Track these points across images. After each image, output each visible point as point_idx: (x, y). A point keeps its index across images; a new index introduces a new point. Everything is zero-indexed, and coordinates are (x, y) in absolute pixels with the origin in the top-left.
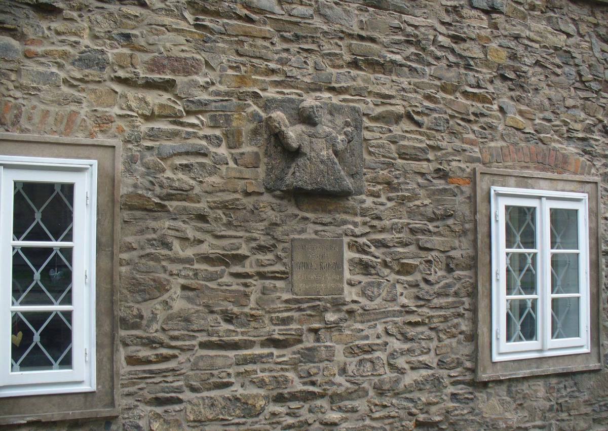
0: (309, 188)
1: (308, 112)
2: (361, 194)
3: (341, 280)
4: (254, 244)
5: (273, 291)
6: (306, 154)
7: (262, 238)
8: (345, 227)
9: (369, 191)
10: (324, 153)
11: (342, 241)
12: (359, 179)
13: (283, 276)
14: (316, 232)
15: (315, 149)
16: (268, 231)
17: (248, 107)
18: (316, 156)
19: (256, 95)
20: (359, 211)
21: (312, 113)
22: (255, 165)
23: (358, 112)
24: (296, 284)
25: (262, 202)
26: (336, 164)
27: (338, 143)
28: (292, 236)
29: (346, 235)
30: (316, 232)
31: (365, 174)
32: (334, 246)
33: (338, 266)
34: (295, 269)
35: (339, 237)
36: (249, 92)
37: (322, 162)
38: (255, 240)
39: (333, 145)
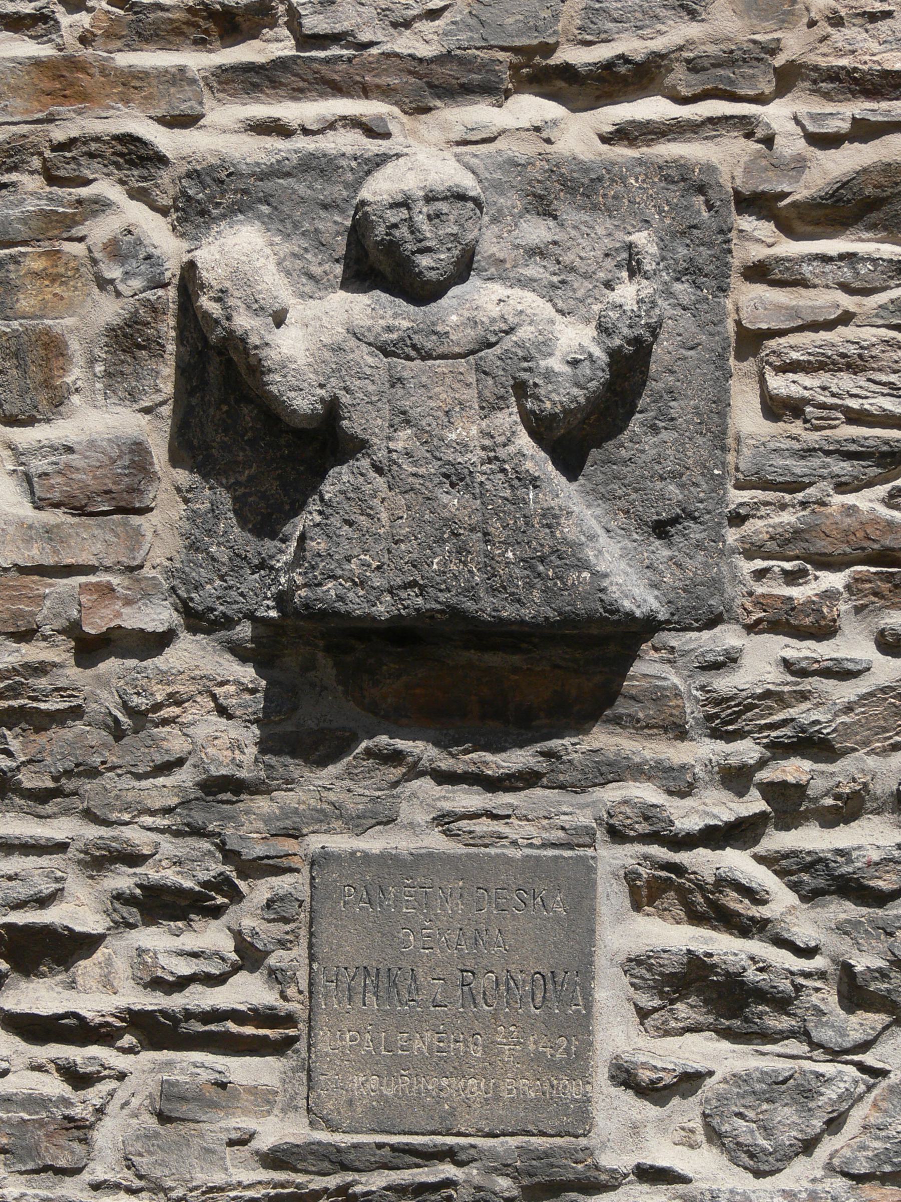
0: (383, 609)
1: (381, 230)
2: (713, 622)
3: (577, 1063)
4: (123, 880)
5: (213, 1105)
6: (360, 446)
7: (168, 846)
8: (612, 794)
9: (760, 602)
10: (467, 430)
11: (588, 868)
12: (699, 546)
13: (266, 1034)
14: (445, 821)
15: (414, 413)
16: (198, 817)
17: (94, 214)
18: (421, 452)
19: (134, 156)
20: (693, 712)
21: (403, 232)
22: (125, 500)
23: (701, 189)
25: (164, 677)
26: (535, 482)
27: (549, 375)
28: (315, 843)
29: (617, 835)
30: (445, 821)
31: (737, 519)
33: (564, 990)
34: (331, 1003)
35: (569, 846)
36: (97, 139)
37: (455, 478)
38: (133, 859)
39: (521, 389)
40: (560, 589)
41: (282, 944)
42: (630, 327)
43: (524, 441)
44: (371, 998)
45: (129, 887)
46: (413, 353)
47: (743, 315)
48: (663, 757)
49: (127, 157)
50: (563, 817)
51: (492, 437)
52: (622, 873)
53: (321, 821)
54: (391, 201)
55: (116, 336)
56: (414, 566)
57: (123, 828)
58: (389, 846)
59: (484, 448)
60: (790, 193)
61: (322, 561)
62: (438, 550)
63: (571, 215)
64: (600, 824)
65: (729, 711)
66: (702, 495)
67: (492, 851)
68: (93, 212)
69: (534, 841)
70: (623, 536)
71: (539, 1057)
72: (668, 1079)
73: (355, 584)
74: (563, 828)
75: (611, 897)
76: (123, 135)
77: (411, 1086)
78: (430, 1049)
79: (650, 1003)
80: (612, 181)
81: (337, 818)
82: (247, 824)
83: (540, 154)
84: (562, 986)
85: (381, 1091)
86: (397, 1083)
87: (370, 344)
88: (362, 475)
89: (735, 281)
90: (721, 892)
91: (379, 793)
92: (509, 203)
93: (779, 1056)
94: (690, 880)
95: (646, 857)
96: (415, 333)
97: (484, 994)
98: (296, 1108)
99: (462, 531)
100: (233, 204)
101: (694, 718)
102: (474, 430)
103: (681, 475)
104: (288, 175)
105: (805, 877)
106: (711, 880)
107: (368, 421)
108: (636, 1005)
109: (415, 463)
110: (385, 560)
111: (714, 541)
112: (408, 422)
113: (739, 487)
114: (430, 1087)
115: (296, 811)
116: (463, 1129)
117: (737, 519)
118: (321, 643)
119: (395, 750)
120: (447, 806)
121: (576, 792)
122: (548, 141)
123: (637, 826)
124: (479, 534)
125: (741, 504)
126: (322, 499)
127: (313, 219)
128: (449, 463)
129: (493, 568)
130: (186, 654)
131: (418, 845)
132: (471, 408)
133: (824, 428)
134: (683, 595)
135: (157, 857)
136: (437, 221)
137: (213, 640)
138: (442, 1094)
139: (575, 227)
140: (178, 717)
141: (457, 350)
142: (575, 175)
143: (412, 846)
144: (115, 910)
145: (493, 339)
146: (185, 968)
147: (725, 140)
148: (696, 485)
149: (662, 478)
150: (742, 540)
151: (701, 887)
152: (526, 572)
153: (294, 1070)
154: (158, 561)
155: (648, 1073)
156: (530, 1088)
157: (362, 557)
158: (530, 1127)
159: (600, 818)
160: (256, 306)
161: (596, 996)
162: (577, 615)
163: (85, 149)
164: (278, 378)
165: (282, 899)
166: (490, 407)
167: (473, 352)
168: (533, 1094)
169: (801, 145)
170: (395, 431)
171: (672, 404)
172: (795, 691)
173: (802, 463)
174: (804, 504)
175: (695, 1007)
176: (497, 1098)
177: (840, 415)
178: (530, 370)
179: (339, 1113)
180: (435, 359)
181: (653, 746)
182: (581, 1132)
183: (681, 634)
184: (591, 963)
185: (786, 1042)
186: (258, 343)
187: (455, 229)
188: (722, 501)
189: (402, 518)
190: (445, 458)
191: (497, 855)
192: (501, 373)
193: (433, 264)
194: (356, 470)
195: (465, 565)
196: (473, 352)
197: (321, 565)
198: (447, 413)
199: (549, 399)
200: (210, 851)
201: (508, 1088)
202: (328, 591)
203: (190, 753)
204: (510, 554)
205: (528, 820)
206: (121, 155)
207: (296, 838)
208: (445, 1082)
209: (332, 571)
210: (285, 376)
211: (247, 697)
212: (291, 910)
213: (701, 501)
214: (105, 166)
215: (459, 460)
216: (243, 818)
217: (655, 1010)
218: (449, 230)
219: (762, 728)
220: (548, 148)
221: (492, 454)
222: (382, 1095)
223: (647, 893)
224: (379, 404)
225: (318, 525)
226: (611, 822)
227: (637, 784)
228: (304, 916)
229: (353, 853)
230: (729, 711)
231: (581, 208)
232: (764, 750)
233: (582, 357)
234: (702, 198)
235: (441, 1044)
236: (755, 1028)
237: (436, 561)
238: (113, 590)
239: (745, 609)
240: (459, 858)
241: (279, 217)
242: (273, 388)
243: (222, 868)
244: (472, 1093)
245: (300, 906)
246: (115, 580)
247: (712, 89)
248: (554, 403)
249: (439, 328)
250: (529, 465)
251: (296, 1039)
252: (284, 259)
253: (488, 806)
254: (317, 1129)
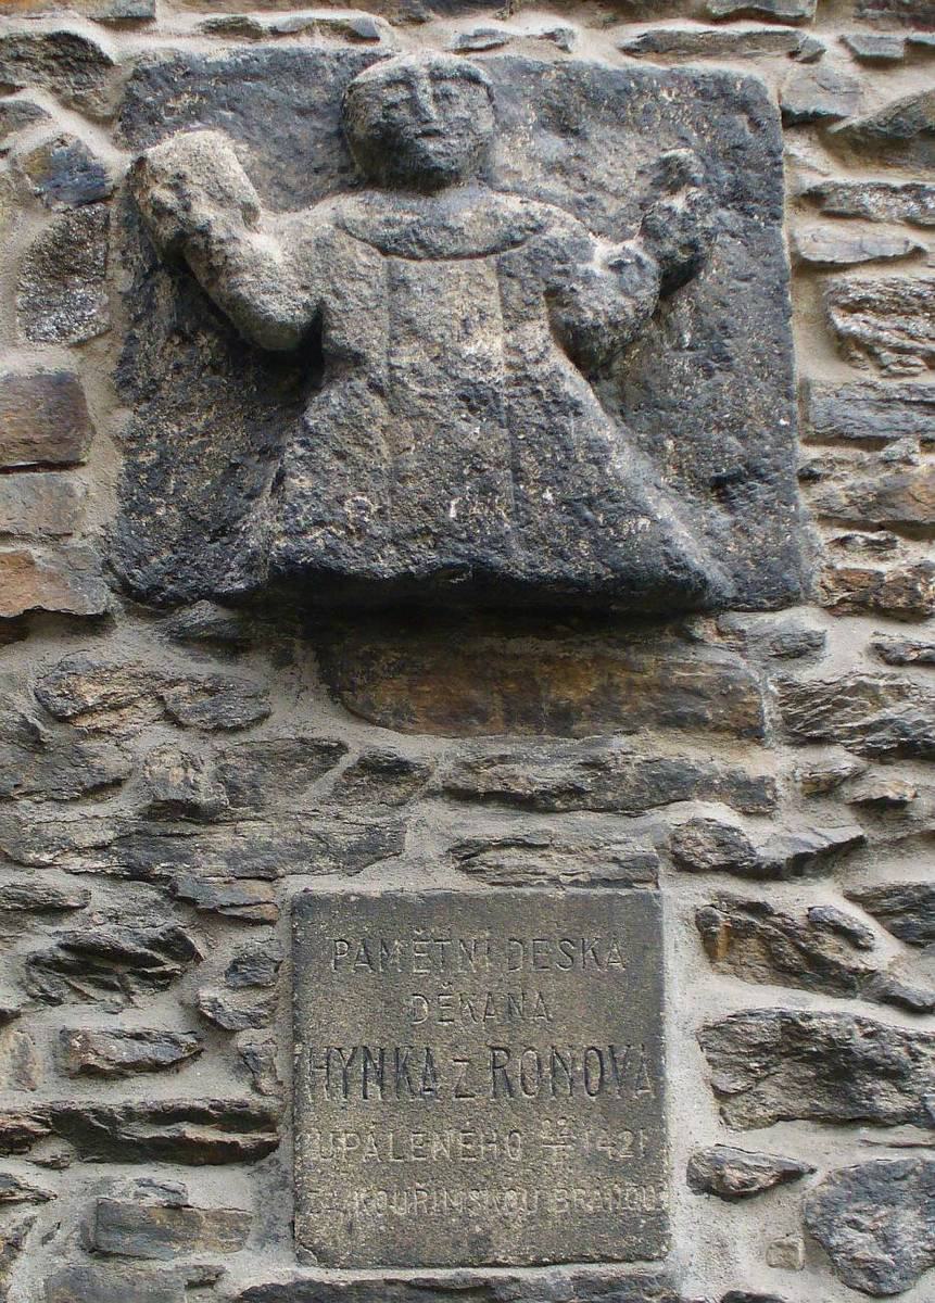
0: (386, 564)
1: (376, 112)
2: (787, 600)
3: (646, 1165)
4: (42, 940)
5: (165, 1235)
6: (357, 360)
7: (103, 897)
8: (675, 816)
9: (841, 580)
10: (490, 343)
12: (767, 508)
14: (466, 855)
15: (421, 322)
16: (141, 855)
17: (20, 125)
18: (432, 370)
19: (71, 56)
20: (770, 712)
21: (403, 114)
23: (744, 106)
24: (319, 1192)
25: (98, 674)
26: (575, 408)
27: (587, 279)
28: (294, 886)
29: (684, 866)
30: (466, 855)
31: (809, 477)
32: (593, 937)
34: (320, 1097)
35: (628, 883)
36: (27, 40)
37: (475, 400)
38: (53, 910)
39: (554, 295)
40: (613, 539)
41: (254, 1020)
42: (683, 230)
43: (559, 360)
44: (374, 1088)
45: (51, 950)
46: (419, 252)
47: (801, 245)
48: (736, 767)
49: (63, 61)
50: (614, 847)
51: (521, 352)
52: (692, 916)
53: (302, 859)
54: (388, 79)
55: (43, 260)
56: (426, 509)
57: (42, 872)
58: (392, 888)
59: (510, 365)
60: (843, 118)
61: (307, 503)
62: (456, 489)
63: (596, 132)
64: (664, 854)
65: (815, 711)
66: (767, 448)
67: (528, 891)
68: (18, 121)
69: (581, 878)
70: (675, 495)
71: (595, 1159)
72: (764, 1179)
73: (350, 532)
74: (616, 860)
75: (679, 951)
76: (59, 34)
77: (429, 1205)
78: (453, 1153)
79: (733, 1086)
80: (641, 93)
81: (323, 853)
82: (205, 865)
83: (556, 63)
84: (625, 1064)
85: (389, 1210)
86: (411, 1200)
87: (364, 240)
88: (358, 396)
89: (787, 210)
90: (816, 938)
91: (378, 820)
92: (522, 112)
93: (892, 1146)
94: (775, 925)
95: (721, 896)
96: (421, 227)
97: (523, 1078)
98: (277, 1238)
99: (486, 466)
100: (191, 108)
101: (771, 720)
102: (498, 344)
103: (742, 424)
104: (256, 77)
105: (913, 919)
106: (801, 922)
107: (363, 330)
108: (714, 1088)
109: (425, 383)
110: (388, 503)
111: (785, 504)
112: (414, 333)
113: (809, 441)
114: (455, 1204)
115: (268, 847)
116: (500, 1259)
117: (809, 477)
118: (299, 628)
119: (398, 761)
120: (467, 835)
121: (629, 815)
122: (564, 48)
123: (709, 856)
124: (509, 471)
125: (815, 461)
126: (306, 428)
127: (288, 125)
128: (468, 382)
129: (527, 513)
130: (125, 647)
131: (430, 886)
132: (493, 316)
133: (903, 375)
134: (753, 567)
135: (87, 910)
136: (446, 103)
137: (160, 630)
138: (472, 1213)
139: (600, 141)
140: (115, 726)
141: (474, 247)
142: (598, 85)
143: (422, 887)
144: (32, 980)
145: (518, 236)
146: (123, 1052)
147: (765, 60)
148: (760, 436)
149: (720, 428)
150: (817, 504)
151: (789, 932)
152: (569, 518)
153: (272, 1188)
154: (90, 529)
155: (738, 1174)
156: (587, 1200)
157: (359, 498)
158: (590, 1252)
159: (663, 847)
160: (220, 195)
161: (668, 1074)
162: (635, 572)
163: (11, 52)
164: (248, 277)
165: (252, 961)
166: (515, 319)
167: (494, 251)
168: (591, 1208)
169: (851, 71)
170: (398, 343)
171: (726, 341)
172: (892, 686)
173: (882, 415)
174: (887, 463)
175: (786, 1088)
176: (545, 1216)
177: (920, 362)
178: (565, 273)
179: (335, 1242)
180: (447, 258)
181: (725, 755)
182: (655, 1254)
183: (750, 615)
184: (660, 1032)
185: (900, 1128)
186: (224, 236)
187: (467, 114)
188: (790, 457)
189: (409, 449)
190: (464, 375)
191: (533, 895)
192: (530, 275)
193: (442, 149)
194: (348, 392)
195: (492, 508)
196: (494, 251)
197: (305, 508)
198: (464, 323)
199: (591, 308)
200: (156, 901)
201: (556, 1200)
202: (314, 541)
203: (130, 773)
204: (548, 496)
205: (570, 852)
206: (55, 57)
207: (270, 880)
208: (474, 1196)
209: (319, 515)
210: (258, 276)
211: (204, 699)
212: (266, 974)
213: (767, 456)
214: (36, 71)
215: (481, 379)
216: (199, 857)
217: (739, 1093)
218: (459, 114)
219: (853, 732)
220: (565, 57)
221: (520, 373)
222: (392, 1217)
223: (721, 939)
224: (377, 311)
225: (301, 458)
226: (678, 850)
227: (707, 803)
228: (283, 982)
229: (346, 898)
230: (815, 711)
231: (604, 122)
232: (858, 759)
233: (629, 261)
234: (745, 117)
235: (469, 1147)
236: (864, 1112)
237: (453, 503)
238: (32, 563)
239: (824, 587)
240: (483, 900)
241: (244, 126)
242: (243, 291)
243: (172, 922)
244: (511, 1210)
245: (276, 970)
246: (36, 552)
247: (747, 9)
248: (597, 313)
249: (451, 222)
250: (567, 387)
251: (272, 1147)
252: (252, 168)
253: (520, 834)
254: (307, 1264)
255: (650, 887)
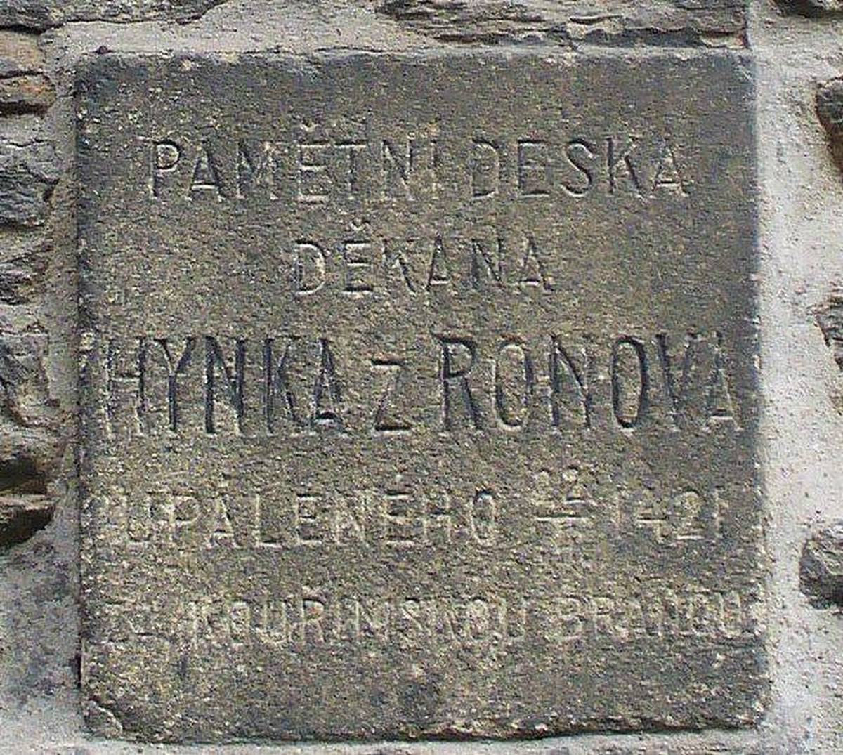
3: (726, 555)
11: (734, 84)
24: (125, 604)
32: (628, 137)
34: (128, 432)
35: (691, 38)
44: (225, 412)
52: (809, 98)
58: (259, 47)
67: (508, 52)
69: (605, 27)
71: (631, 543)
77: (327, 625)
78: (372, 529)
84: (686, 368)
85: (253, 636)
86: (294, 618)
97: (500, 395)
98: (48, 687)
114: (375, 625)
116: (458, 726)
131: (329, 42)
138: (407, 642)
143: (314, 44)
153: (40, 596)
156: (616, 617)
158: (623, 712)
161: (765, 387)
168: (624, 633)
176: (539, 647)
179: (155, 695)
184: (751, 311)
191: (520, 60)
201: (561, 619)
207: (36, 32)
208: (410, 611)
212: (29, 204)
222: (259, 648)
228: (59, 218)
235: (400, 520)
240: (428, 69)
244: (477, 635)
245: (47, 196)
251: (41, 520)
254: (104, 736)
255: (733, 44)
